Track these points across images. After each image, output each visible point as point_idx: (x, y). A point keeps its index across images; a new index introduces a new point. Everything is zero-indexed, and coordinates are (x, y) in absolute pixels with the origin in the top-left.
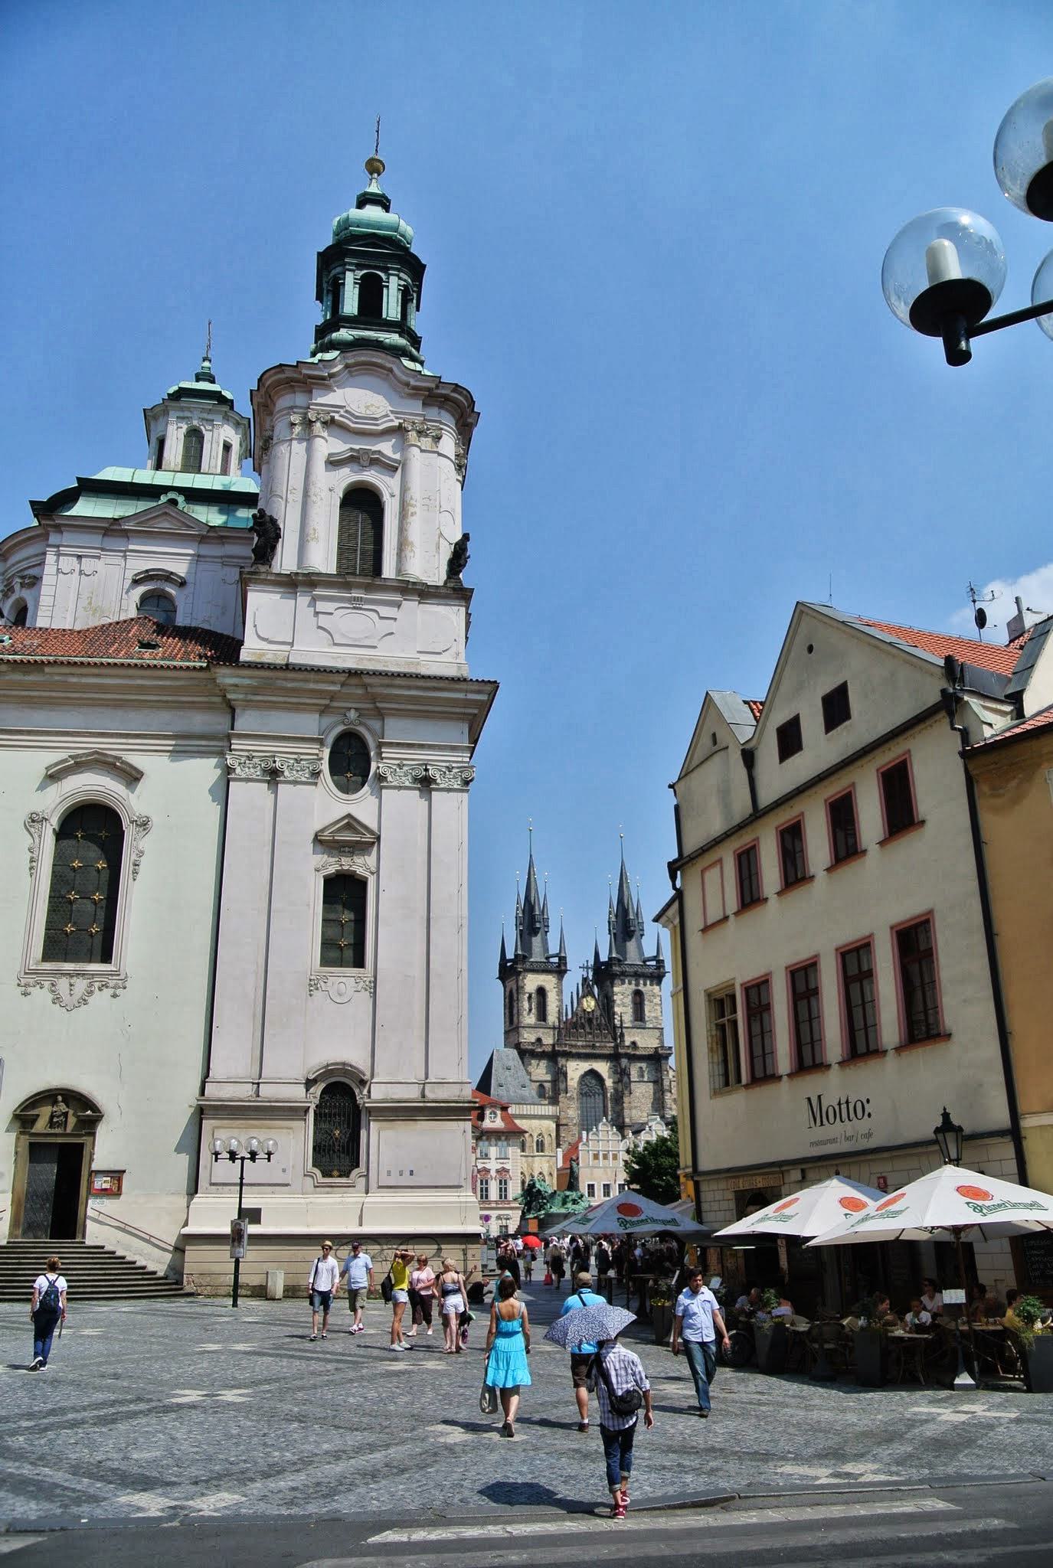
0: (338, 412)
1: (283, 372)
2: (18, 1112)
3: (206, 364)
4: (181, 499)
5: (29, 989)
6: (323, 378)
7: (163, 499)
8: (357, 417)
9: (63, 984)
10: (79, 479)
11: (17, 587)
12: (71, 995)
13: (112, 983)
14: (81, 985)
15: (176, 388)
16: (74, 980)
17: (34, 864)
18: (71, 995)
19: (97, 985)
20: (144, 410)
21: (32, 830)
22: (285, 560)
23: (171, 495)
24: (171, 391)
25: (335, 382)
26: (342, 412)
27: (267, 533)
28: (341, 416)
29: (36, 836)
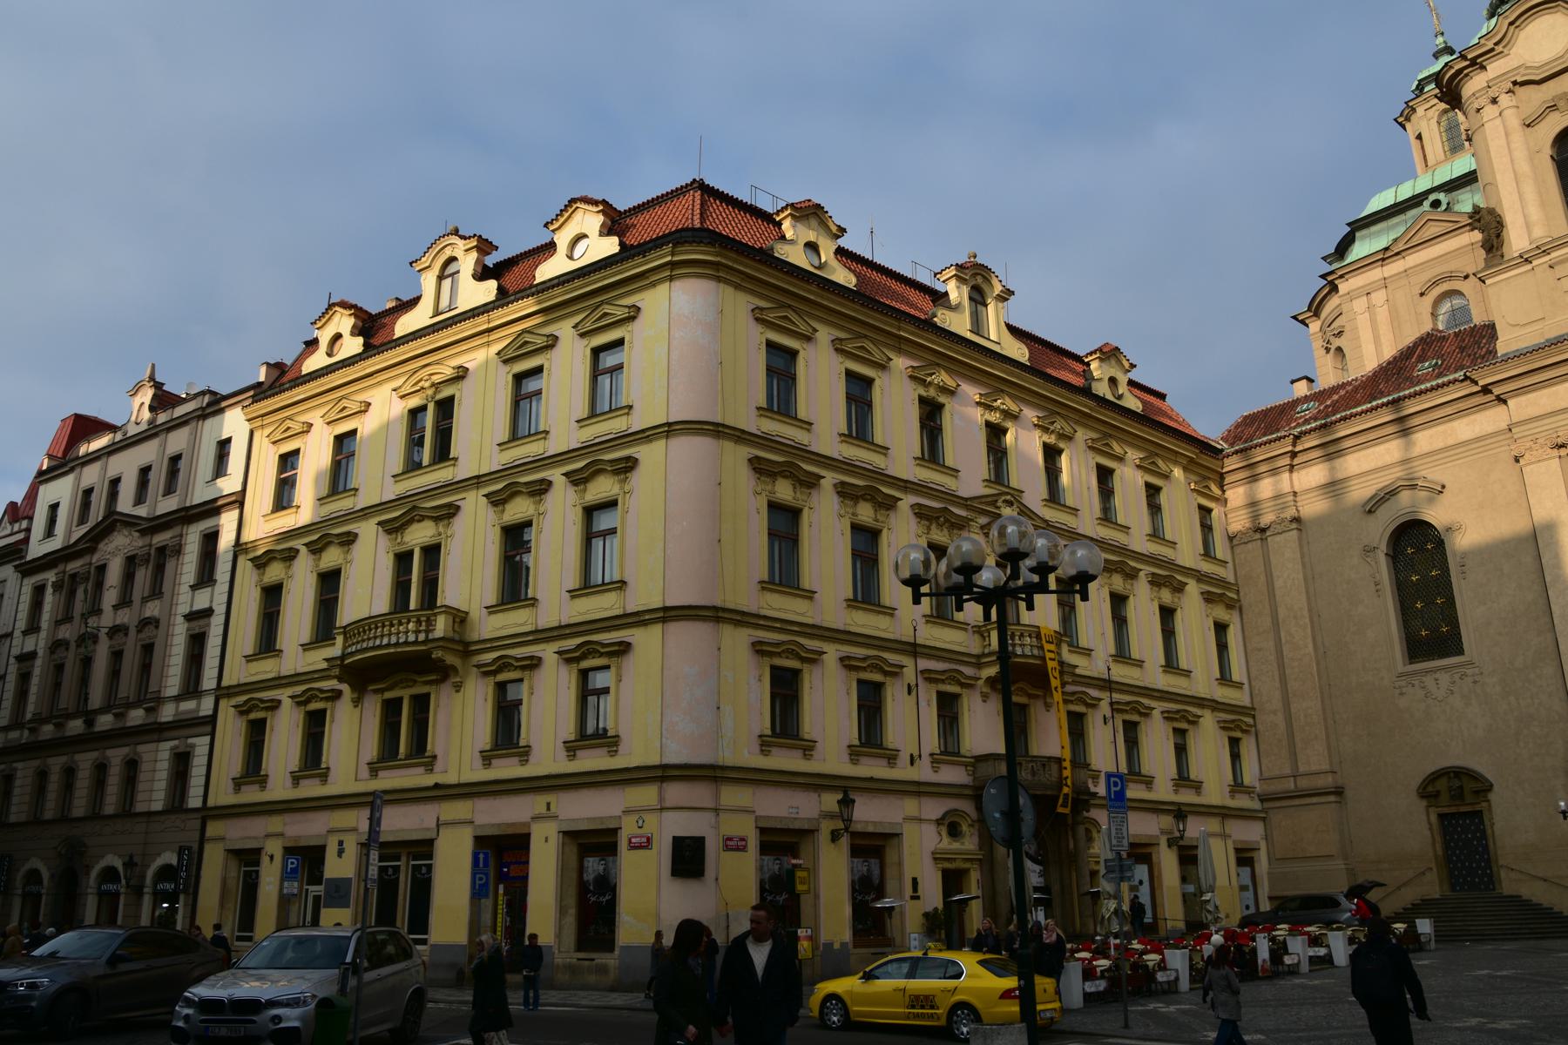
0: (1517, 74)
1: (1451, 67)
2: (1421, 791)
3: (1440, 40)
4: (1441, 196)
5: (1404, 690)
6: (1492, 50)
7: (1426, 204)
8: (1538, 68)
9: (1428, 680)
10: (1349, 224)
11: (1332, 339)
12: (1438, 688)
13: (1469, 672)
14: (1444, 678)
15: (1417, 83)
16: (1437, 675)
17: (1378, 587)
18: (1438, 688)
19: (1457, 677)
20: (1395, 120)
21: (1369, 560)
22: (1517, 240)
23: (1432, 197)
24: (1414, 87)
25: (1504, 47)
26: (1521, 70)
27: (1489, 225)
28: (1524, 75)
29: (1373, 563)
